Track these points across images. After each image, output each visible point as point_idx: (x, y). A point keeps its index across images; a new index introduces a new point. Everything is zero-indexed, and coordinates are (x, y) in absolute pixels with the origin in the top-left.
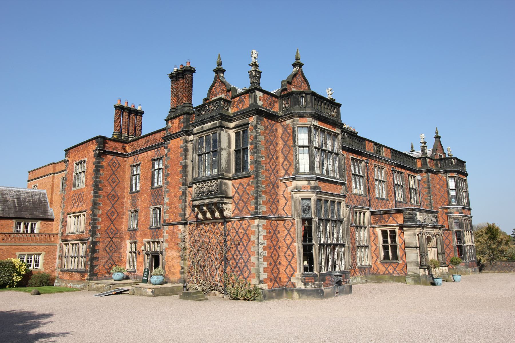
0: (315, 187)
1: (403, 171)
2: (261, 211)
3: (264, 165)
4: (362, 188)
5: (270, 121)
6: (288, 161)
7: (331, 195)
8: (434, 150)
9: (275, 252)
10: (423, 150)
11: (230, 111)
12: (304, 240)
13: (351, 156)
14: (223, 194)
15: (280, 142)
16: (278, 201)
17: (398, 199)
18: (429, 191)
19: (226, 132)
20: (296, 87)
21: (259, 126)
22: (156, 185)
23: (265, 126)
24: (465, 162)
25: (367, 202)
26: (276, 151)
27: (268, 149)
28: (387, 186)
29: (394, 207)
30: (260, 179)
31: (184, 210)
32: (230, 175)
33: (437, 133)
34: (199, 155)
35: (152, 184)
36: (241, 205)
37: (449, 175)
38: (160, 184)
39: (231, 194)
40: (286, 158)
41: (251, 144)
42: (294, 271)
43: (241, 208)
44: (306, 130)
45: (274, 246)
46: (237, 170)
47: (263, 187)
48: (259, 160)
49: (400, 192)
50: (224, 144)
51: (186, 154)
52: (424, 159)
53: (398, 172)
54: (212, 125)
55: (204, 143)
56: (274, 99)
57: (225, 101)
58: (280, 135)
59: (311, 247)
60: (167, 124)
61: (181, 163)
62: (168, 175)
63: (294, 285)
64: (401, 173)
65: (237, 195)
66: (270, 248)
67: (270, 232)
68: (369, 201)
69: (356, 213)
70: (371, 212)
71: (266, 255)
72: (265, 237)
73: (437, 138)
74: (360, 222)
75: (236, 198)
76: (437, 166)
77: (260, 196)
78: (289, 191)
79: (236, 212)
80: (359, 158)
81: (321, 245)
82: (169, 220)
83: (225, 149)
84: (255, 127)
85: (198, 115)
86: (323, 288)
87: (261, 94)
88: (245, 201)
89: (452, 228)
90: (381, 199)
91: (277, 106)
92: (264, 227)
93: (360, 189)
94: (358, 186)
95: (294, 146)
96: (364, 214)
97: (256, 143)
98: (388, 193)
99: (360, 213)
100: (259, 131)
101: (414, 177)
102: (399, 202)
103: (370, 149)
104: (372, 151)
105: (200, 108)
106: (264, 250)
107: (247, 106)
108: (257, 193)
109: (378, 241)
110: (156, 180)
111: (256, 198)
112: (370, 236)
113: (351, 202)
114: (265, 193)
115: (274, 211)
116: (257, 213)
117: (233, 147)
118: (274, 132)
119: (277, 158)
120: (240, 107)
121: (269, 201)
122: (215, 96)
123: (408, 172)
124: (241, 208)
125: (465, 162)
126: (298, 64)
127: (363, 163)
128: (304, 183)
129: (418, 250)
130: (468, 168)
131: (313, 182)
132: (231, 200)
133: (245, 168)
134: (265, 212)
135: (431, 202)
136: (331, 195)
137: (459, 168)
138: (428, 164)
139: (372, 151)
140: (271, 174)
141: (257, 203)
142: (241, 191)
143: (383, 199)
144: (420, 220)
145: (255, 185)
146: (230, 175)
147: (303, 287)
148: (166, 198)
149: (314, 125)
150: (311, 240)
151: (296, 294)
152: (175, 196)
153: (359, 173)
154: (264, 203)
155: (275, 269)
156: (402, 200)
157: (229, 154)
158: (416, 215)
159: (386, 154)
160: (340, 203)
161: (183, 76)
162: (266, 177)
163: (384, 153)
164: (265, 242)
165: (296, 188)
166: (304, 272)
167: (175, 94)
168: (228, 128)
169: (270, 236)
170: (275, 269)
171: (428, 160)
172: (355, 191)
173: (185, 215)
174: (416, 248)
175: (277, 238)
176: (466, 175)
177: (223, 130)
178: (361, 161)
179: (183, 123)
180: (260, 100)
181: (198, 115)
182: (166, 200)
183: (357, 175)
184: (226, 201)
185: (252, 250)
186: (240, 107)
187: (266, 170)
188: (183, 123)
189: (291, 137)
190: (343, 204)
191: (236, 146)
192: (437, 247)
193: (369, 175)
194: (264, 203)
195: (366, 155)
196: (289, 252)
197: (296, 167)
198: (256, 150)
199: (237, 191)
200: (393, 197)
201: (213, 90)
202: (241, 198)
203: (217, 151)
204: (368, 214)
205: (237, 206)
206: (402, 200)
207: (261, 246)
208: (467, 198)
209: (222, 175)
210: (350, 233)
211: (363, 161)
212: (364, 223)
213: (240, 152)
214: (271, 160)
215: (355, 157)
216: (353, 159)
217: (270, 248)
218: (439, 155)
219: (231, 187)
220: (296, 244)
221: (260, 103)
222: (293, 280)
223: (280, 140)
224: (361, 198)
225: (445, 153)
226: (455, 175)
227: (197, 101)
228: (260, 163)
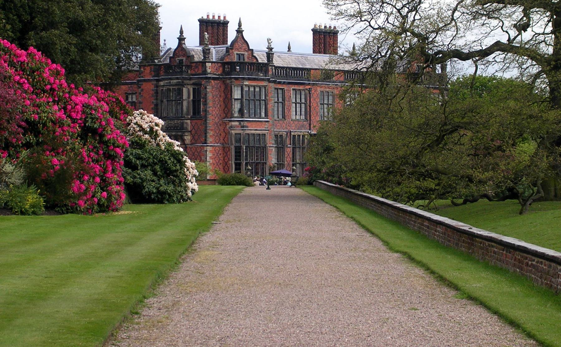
2: (208, 142)
5: (216, 81)
7: (256, 130)
19: (187, 87)
21: (208, 87)
25: (308, 125)
32: (189, 117)
36: (196, 137)
41: (203, 98)
44: (240, 88)
46: (194, 113)
50: (185, 97)
51: (157, 96)
61: (153, 102)
68: (310, 124)
75: (193, 132)
84: (206, 88)
94: (298, 113)
95: (231, 99)
111: (206, 134)
114: (212, 130)
115: (217, 141)
121: (214, 135)
128: (237, 123)
136: (256, 130)
141: (206, 136)
154: (211, 136)
157: (188, 103)
164: (211, 160)
172: (294, 118)
184: (186, 134)
188: (154, 71)
189: (229, 93)
196: (226, 167)
198: (205, 104)
199: (194, 128)
202: (196, 133)
205: (193, 137)
207: (208, 163)
209: (184, 117)
210: (286, 153)
215: (296, 87)
216: (293, 89)
217: (214, 164)
221: (209, 71)
224: (301, 122)
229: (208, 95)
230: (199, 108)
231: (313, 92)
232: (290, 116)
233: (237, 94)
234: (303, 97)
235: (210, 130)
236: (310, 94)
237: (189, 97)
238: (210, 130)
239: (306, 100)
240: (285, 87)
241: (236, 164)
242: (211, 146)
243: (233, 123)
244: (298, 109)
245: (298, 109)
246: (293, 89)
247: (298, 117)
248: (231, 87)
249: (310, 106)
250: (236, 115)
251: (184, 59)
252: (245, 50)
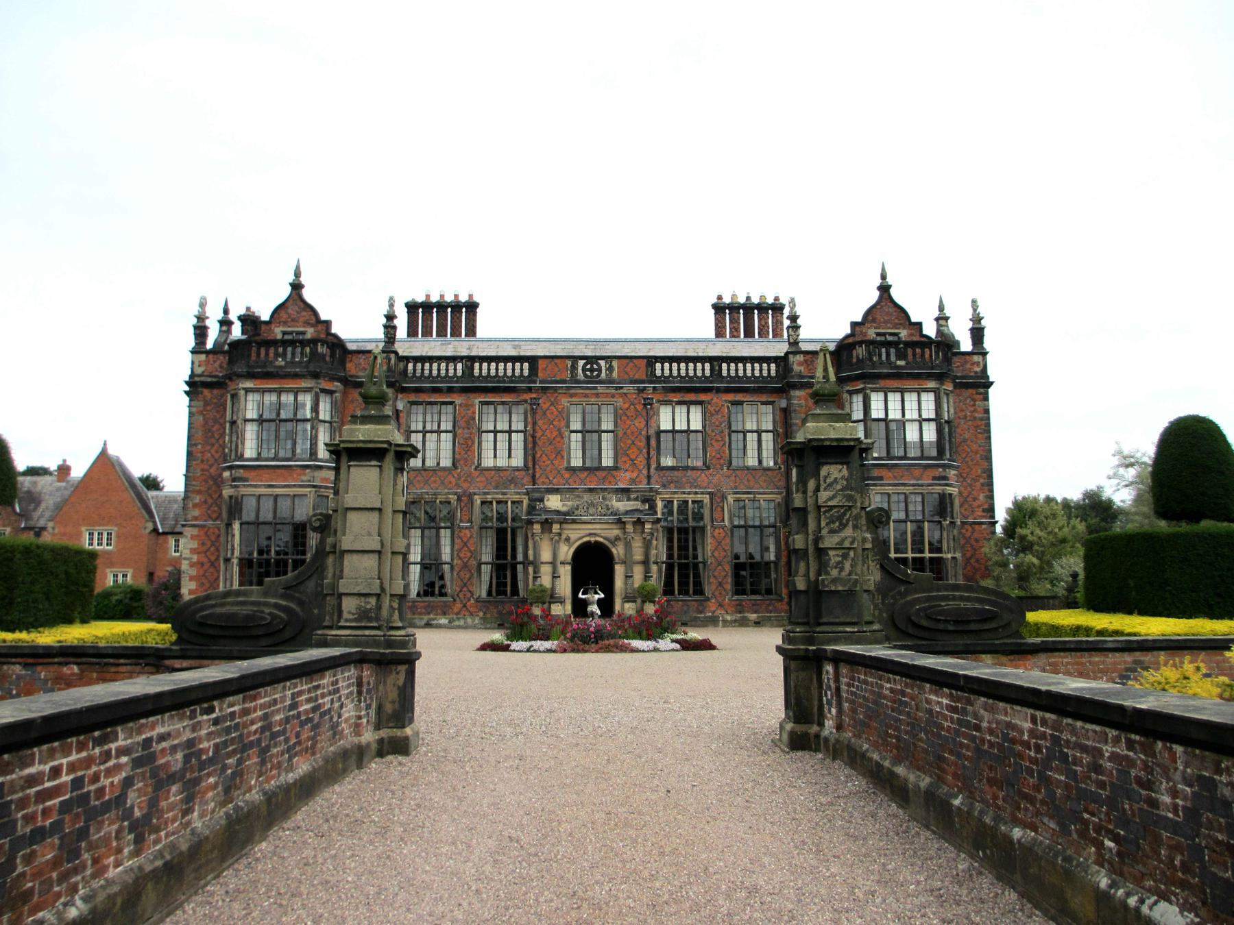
29: (645, 481)
66: (202, 564)
67: (203, 544)
71: (194, 573)
72: (193, 551)
113: (465, 485)
114: (199, 492)
121: (205, 502)
134: (196, 518)
140: (211, 466)
156: (699, 463)
162: (203, 470)
169: (204, 548)
172: (488, 462)
194: (195, 506)
206: (699, 463)
211: (526, 401)
214: (213, 445)
247: (502, 462)
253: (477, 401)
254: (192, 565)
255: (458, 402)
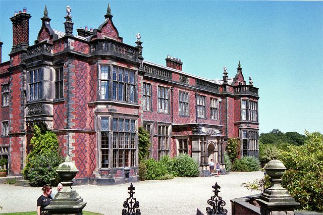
0: (111, 110)
1: (207, 95)
3: (74, 94)
4: (167, 108)
6: (94, 91)
8: (235, 79)
9: (82, 154)
10: (225, 78)
11: (52, 52)
12: (103, 146)
13: (158, 84)
14: (45, 115)
15: (89, 76)
16: (86, 119)
17: (199, 116)
18: (226, 110)
19: (49, 68)
20: (106, 34)
22: (4, 105)
23: (76, 66)
24: (258, 89)
26: (85, 83)
27: (77, 82)
28: (190, 107)
30: (70, 103)
31: (23, 124)
32: (52, 100)
33: (239, 66)
34: (30, 85)
35: (2, 104)
37: (242, 98)
38: (8, 104)
39: (52, 114)
40: (92, 89)
41: (65, 78)
42: (95, 167)
43: (58, 124)
44: (107, 69)
45: (81, 150)
46: (57, 97)
47: (72, 110)
48: (70, 90)
49: (201, 111)
50: (46, 76)
52: (224, 86)
53: (202, 96)
54: (38, 62)
55: (33, 76)
56: (85, 44)
57: (48, 45)
58: (89, 71)
59: (107, 151)
60: (11, 58)
62: (12, 98)
63: (94, 176)
64: (205, 97)
65: (56, 114)
66: (78, 151)
68: (172, 118)
69: (160, 127)
70: (172, 126)
72: (73, 144)
73: (239, 69)
74: (163, 133)
75: (55, 117)
76: (235, 91)
77: (70, 116)
78: (94, 112)
79: (55, 127)
80: (165, 86)
81: (115, 151)
82: (13, 131)
83: (47, 81)
84: (68, 66)
85: (30, 54)
86: (114, 178)
87: (73, 41)
88: (61, 119)
89: (241, 138)
90: (183, 116)
91: (87, 49)
92: (73, 137)
93: (165, 109)
95: (97, 80)
96: (167, 128)
97: (68, 78)
98: (190, 112)
99: (164, 127)
100: (71, 69)
101: (217, 100)
102: (200, 118)
103: (176, 79)
104: (178, 81)
105: (33, 47)
106: (73, 153)
107: (62, 50)
108: (68, 114)
109: (176, 148)
110: (5, 101)
111: (68, 117)
112: (170, 143)
114: (75, 113)
116: (68, 128)
117: (54, 80)
118: (83, 70)
119: (86, 88)
120: (59, 50)
122: (43, 39)
123: (210, 96)
124: (58, 124)
125: (258, 89)
126: (109, 16)
127: (169, 90)
129: (200, 153)
130: (260, 94)
131: (110, 106)
132: (52, 118)
133: (62, 97)
134: (74, 127)
135: (226, 118)
137: (252, 94)
138: (227, 90)
139: (178, 81)
140: (80, 100)
142: (58, 111)
143: (186, 116)
144: (205, 132)
145: (67, 108)
146: (52, 100)
147: (100, 177)
148: (11, 115)
149: (113, 65)
150: (107, 146)
151: (95, 182)
152: (17, 114)
153: (165, 97)
155: (82, 166)
157: (51, 84)
158: (201, 129)
159: (190, 82)
160: (135, 121)
161: (21, 21)
163: (189, 82)
164: (74, 148)
165: (98, 110)
166: (102, 167)
167: (16, 35)
168: (50, 65)
170: (82, 166)
171: (227, 87)
172: (161, 111)
173: (23, 127)
174: (198, 152)
175: (85, 145)
176: (258, 98)
177: (46, 67)
178: (168, 88)
179: (21, 58)
180: (72, 45)
181: (30, 54)
182: (11, 116)
183: (163, 99)
185: (65, 153)
186: (59, 50)
187: (76, 97)
188: (21, 58)
189: (96, 74)
190: (137, 122)
191: (57, 78)
192: (218, 151)
193: (174, 99)
194: (74, 120)
195: (171, 84)
196: (92, 154)
197: (98, 95)
200: (194, 114)
201: (41, 35)
203: (41, 82)
204: (170, 128)
206: (203, 117)
208: (256, 116)
209: (45, 100)
210: (153, 141)
211: (169, 88)
212: (167, 133)
213: (59, 84)
214: (80, 89)
216: (159, 86)
218: (239, 83)
219: (51, 109)
220: (96, 149)
221: (72, 48)
222: (94, 173)
223: (89, 75)
225: (245, 81)
226: (247, 98)
227: (32, 43)
228: (71, 93)
229: (70, 74)
230: (62, 90)
231: (174, 91)
232: (156, 108)
233: (104, 76)
234: (167, 94)
235: (72, 113)
236: (172, 92)
237: (51, 79)
238: (72, 113)
239: (169, 98)
240: (152, 83)
241: (103, 151)
242: (74, 131)
243: (99, 107)
244: (163, 105)
245: (163, 105)
246: (159, 86)
248: (98, 67)
249: (172, 103)
250: (103, 97)
251: (48, 40)
252: (114, 36)
253: (157, 85)
254: (73, 152)
255: (152, 84)
